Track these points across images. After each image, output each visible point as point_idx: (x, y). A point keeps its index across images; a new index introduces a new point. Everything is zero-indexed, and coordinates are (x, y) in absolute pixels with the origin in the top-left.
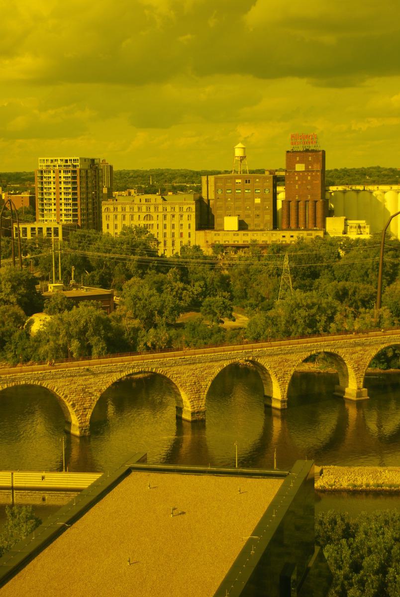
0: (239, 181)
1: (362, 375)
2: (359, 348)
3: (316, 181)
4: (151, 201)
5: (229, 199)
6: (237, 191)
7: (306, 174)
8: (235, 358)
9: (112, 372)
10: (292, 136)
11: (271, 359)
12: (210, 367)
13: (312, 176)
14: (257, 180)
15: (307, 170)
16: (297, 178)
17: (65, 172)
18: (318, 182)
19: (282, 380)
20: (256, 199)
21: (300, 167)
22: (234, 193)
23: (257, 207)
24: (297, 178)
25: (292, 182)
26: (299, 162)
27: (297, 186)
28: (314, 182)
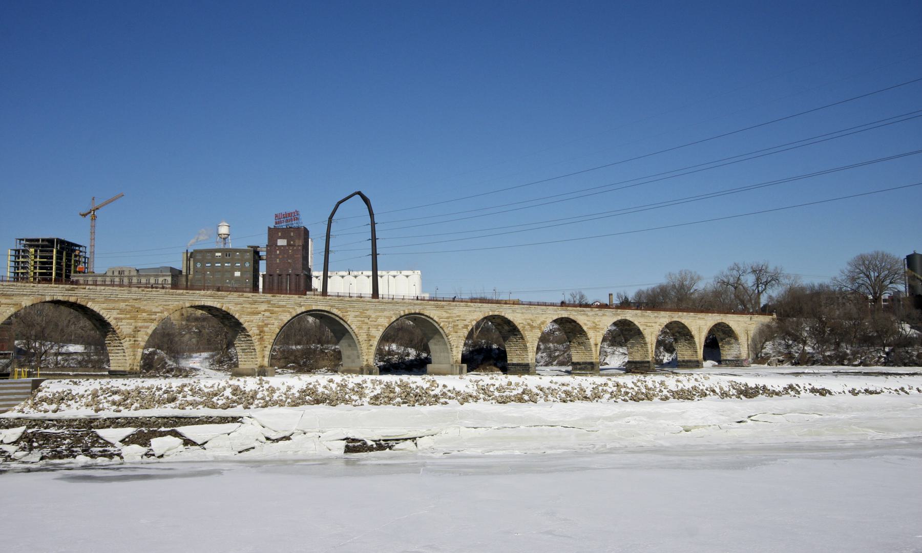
0: (219, 254)
3: (297, 255)
5: (208, 273)
10: (276, 216)
13: (293, 250)
14: (238, 254)
15: (289, 244)
16: (278, 252)
18: (299, 256)
20: (235, 273)
21: (282, 242)
22: (213, 265)
23: (237, 279)
24: (278, 252)
25: (273, 256)
26: (281, 238)
27: (278, 260)
28: (296, 256)
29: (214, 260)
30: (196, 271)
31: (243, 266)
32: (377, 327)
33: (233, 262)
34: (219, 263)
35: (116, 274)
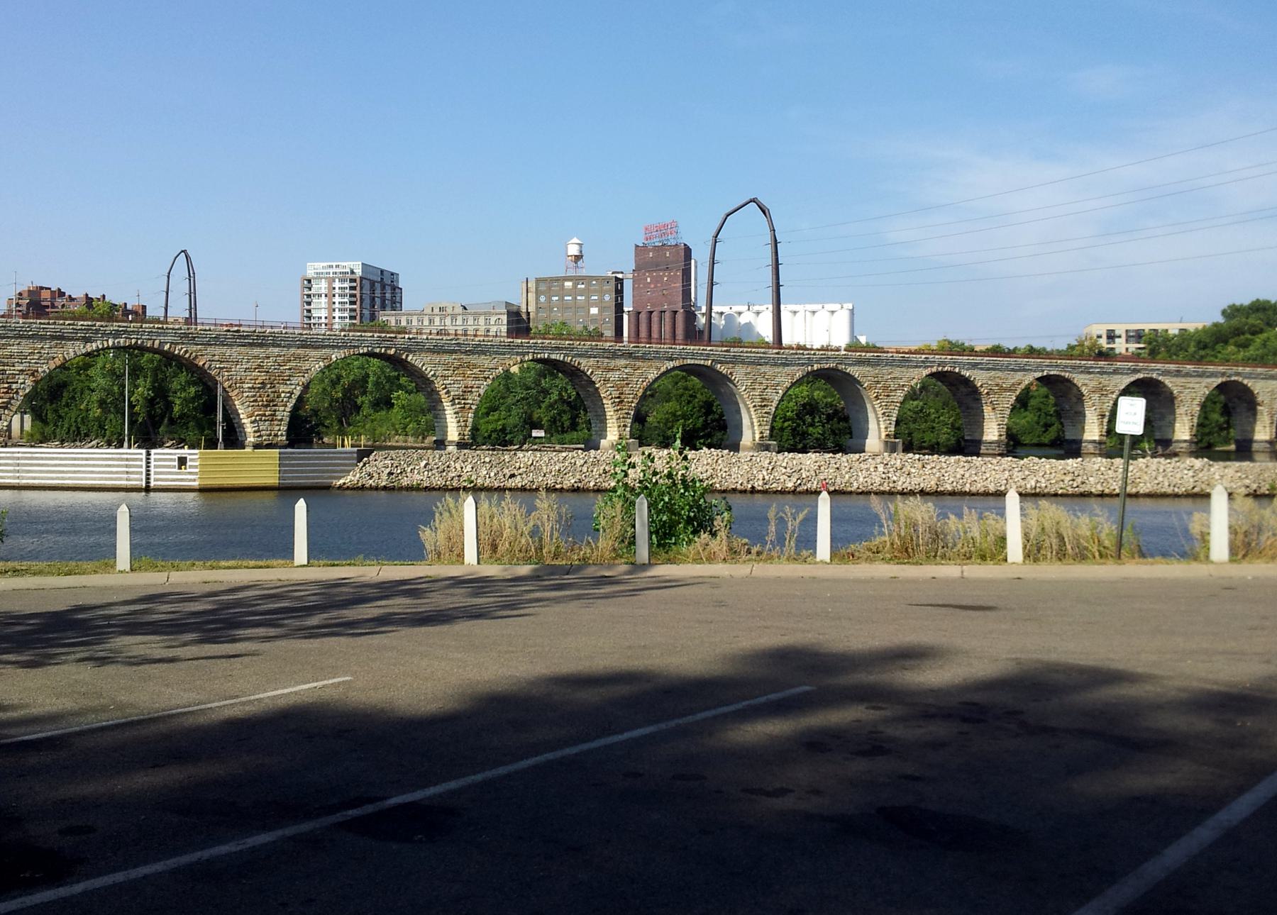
1: (627, 414)
2: (623, 362)
4: (447, 309)
6: (566, 298)
7: (661, 274)
8: (358, 347)
9: (62, 338)
11: (437, 358)
12: (297, 358)
14: (594, 282)
16: (649, 280)
17: (342, 281)
18: (678, 285)
19: (459, 403)
20: (591, 309)
24: (649, 280)
25: (641, 286)
29: (562, 292)
30: (538, 308)
31: (601, 300)
33: (587, 293)
34: (570, 296)
35: (436, 311)
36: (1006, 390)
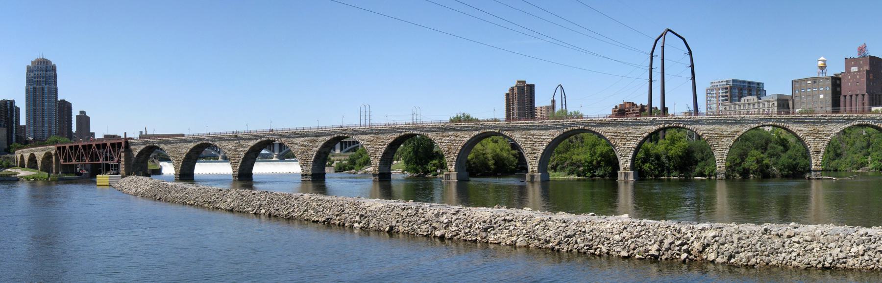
1: (453, 159)
6: (808, 90)
8: (334, 134)
11: (364, 137)
19: (373, 156)
23: (821, 101)
31: (825, 89)
32: (541, 143)
36: (725, 136)
